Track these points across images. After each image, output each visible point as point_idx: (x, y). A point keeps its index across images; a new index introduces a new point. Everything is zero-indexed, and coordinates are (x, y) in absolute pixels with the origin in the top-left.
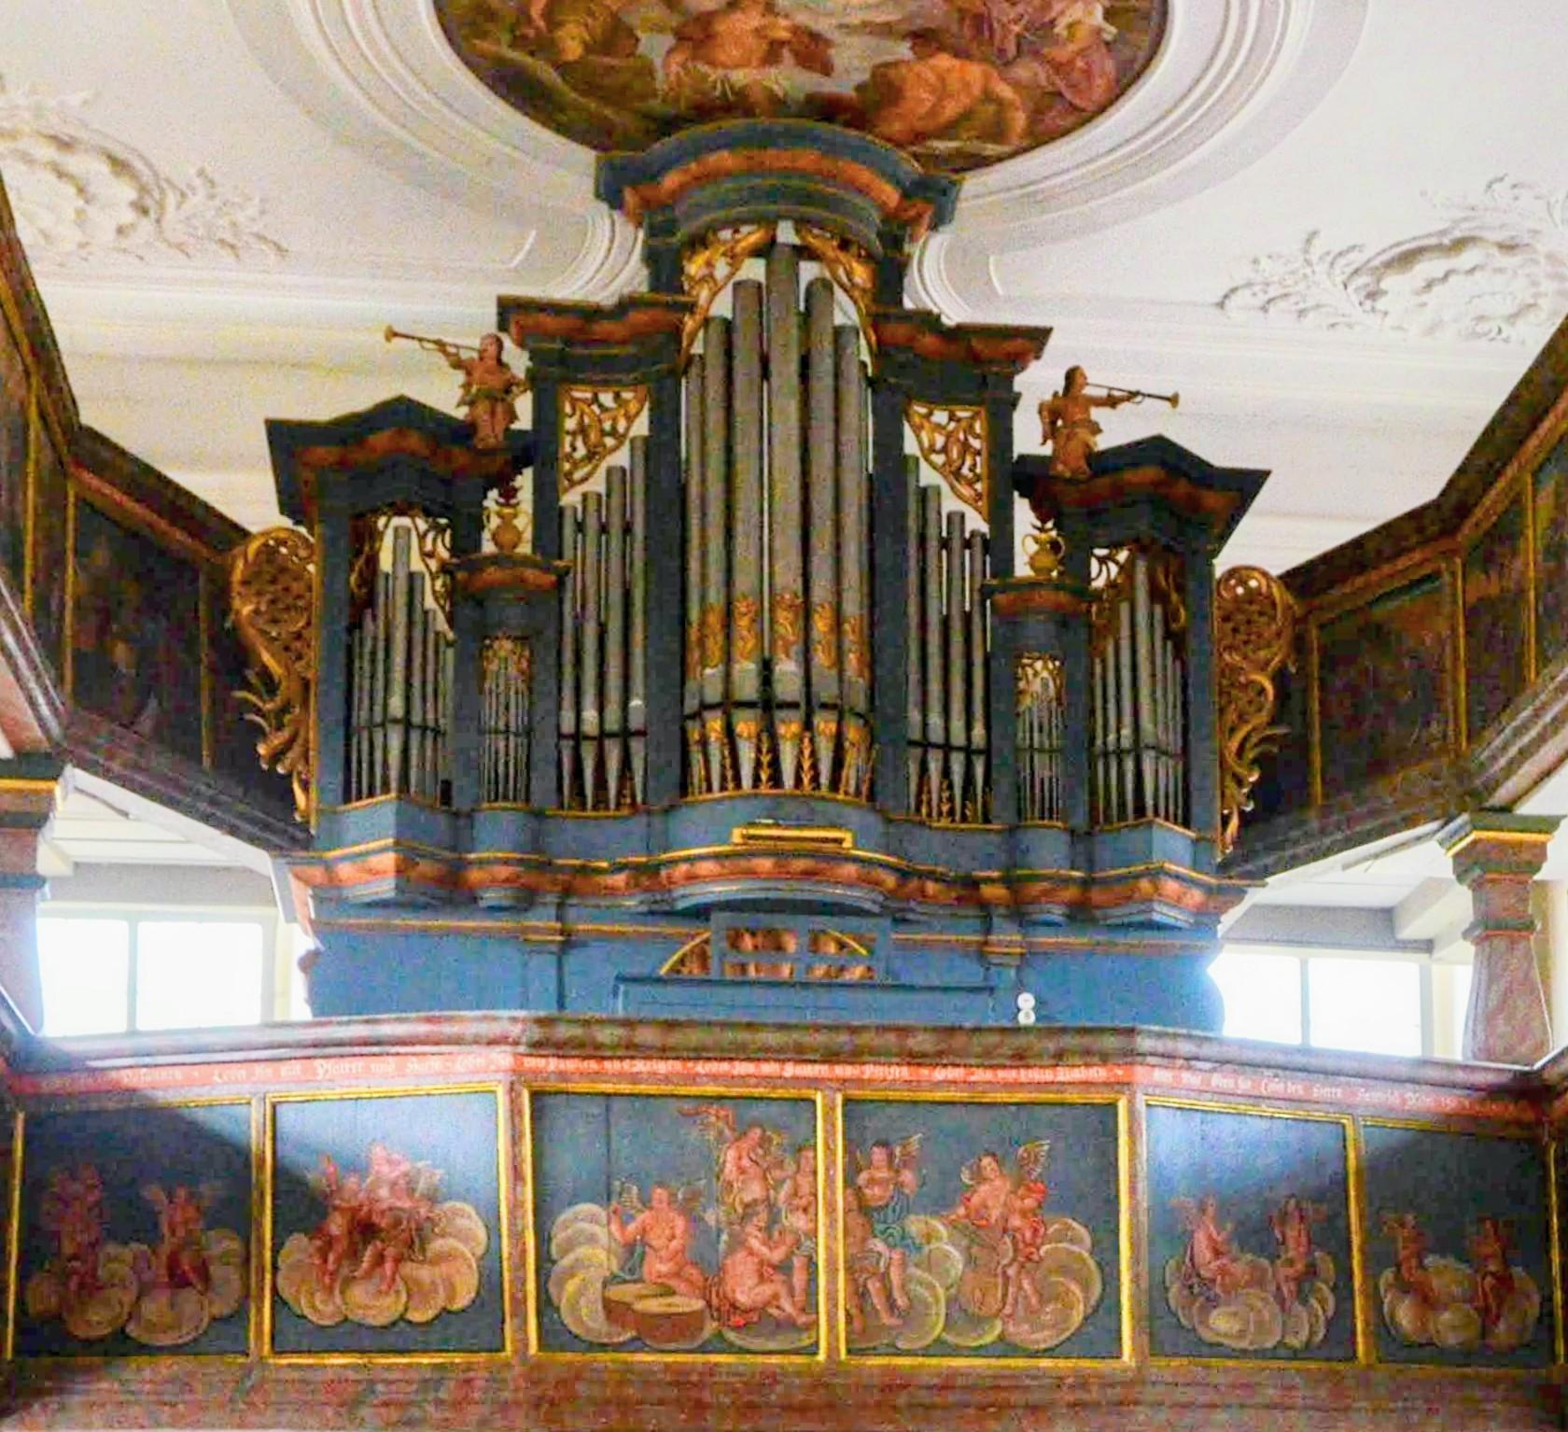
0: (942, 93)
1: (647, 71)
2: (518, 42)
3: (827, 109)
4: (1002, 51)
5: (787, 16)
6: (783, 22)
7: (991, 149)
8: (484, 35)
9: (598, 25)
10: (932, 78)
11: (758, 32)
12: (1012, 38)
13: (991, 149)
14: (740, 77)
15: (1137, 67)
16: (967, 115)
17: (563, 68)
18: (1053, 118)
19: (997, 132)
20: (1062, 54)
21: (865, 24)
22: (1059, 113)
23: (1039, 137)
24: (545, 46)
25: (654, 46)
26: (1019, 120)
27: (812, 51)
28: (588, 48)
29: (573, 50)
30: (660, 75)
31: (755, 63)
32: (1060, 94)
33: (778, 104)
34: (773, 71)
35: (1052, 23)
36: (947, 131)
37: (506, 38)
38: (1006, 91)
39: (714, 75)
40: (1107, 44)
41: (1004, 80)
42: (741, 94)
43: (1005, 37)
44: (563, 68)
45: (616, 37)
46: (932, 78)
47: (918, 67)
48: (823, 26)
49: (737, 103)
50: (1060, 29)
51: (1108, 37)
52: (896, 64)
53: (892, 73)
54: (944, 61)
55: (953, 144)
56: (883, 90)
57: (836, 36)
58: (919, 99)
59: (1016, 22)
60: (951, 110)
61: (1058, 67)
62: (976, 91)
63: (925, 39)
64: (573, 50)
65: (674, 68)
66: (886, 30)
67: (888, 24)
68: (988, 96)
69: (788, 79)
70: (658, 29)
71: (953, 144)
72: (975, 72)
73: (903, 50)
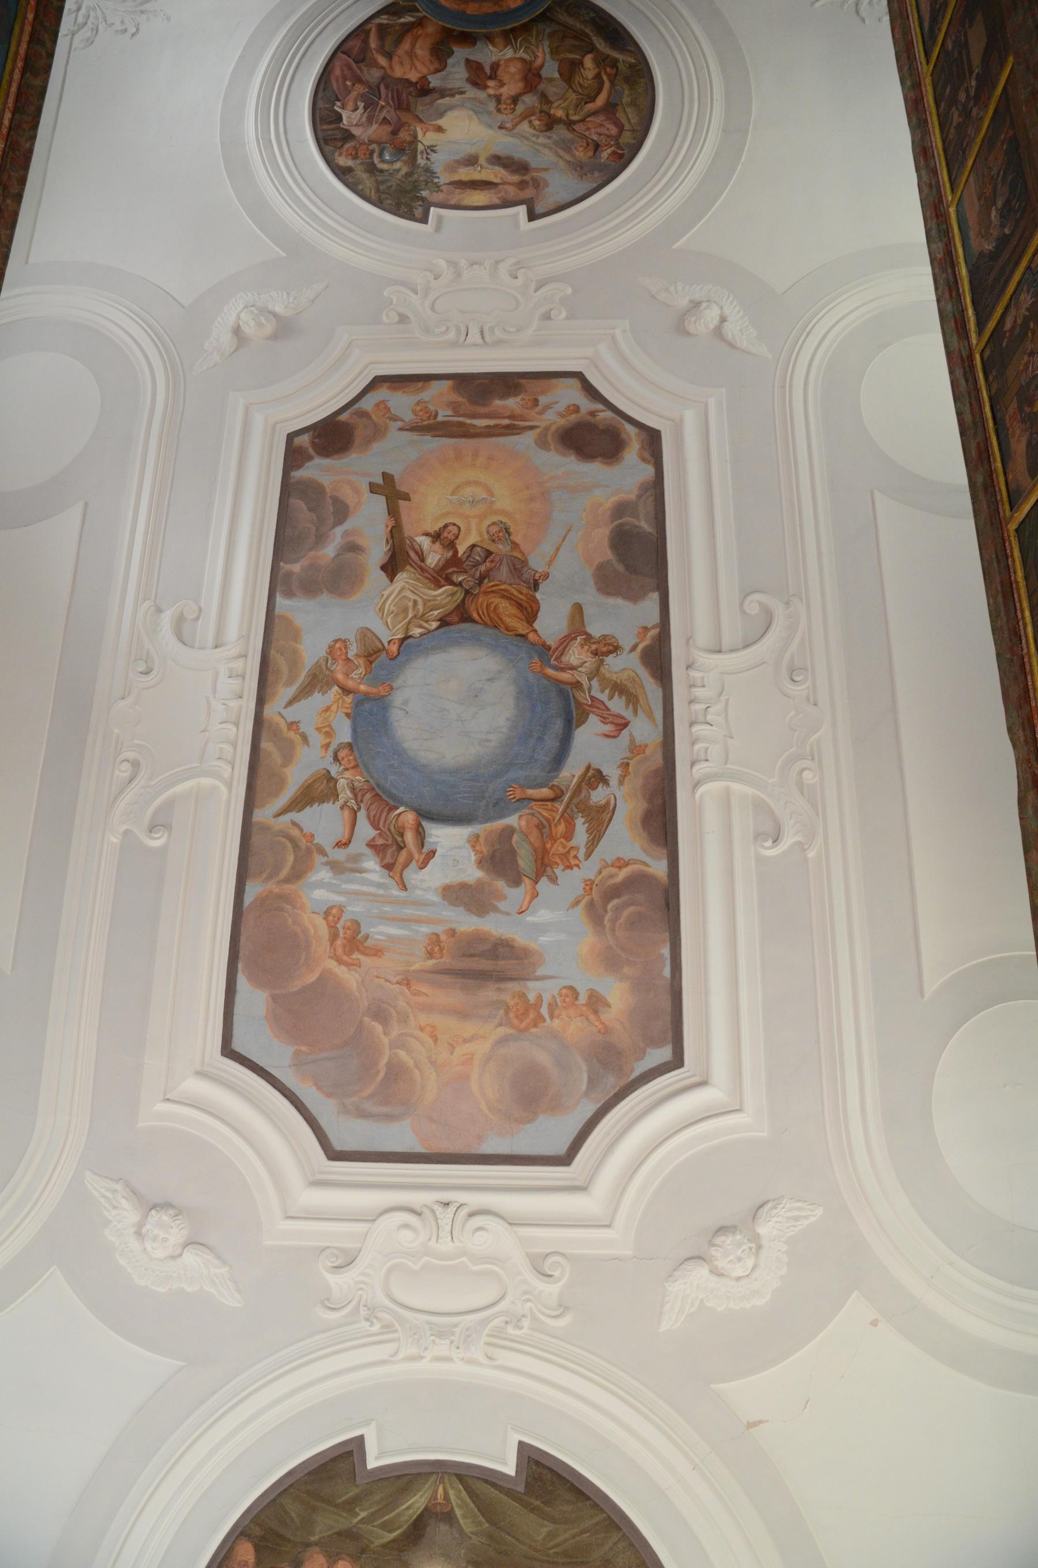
0: (411, 54)
1: (554, 52)
2: (614, 63)
3: (468, 39)
4: (387, 87)
5: (490, 96)
6: (491, 91)
7: (384, 20)
8: (631, 66)
9: (577, 79)
10: (419, 65)
11: (502, 84)
12: (383, 97)
13: (384, 20)
14: (509, 53)
15: (321, 87)
16: (398, 42)
17: (592, 49)
18: (356, 44)
19: (383, 31)
20: (359, 89)
21: (453, 95)
22: (353, 50)
23: (360, 32)
24: (602, 61)
25: (551, 70)
26: (373, 43)
27: (478, 75)
28: (581, 63)
29: (588, 61)
30: (547, 50)
31: (502, 62)
32: (357, 62)
33: (489, 38)
34: (494, 59)
35: (365, 108)
36: (408, 28)
37: (621, 66)
38: (382, 61)
39: (521, 54)
40: (338, 100)
41: (383, 68)
42: (508, 42)
43: (387, 96)
44: (592, 49)
45: (570, 70)
46: (419, 65)
47: (425, 71)
48: (472, 92)
49: (510, 36)
50: (361, 105)
51: (338, 104)
52: (437, 71)
53: (436, 65)
54: (413, 76)
55: (402, 20)
56: (440, 54)
57: (468, 87)
58: (422, 51)
59: (383, 107)
60: (406, 45)
61: (358, 80)
62: (396, 59)
63: (424, 90)
64: (588, 61)
65: (540, 54)
66: (443, 93)
67: (443, 96)
68: (389, 56)
69: (487, 54)
70: (551, 80)
71: (402, 20)
72: (398, 72)
73: (434, 81)
